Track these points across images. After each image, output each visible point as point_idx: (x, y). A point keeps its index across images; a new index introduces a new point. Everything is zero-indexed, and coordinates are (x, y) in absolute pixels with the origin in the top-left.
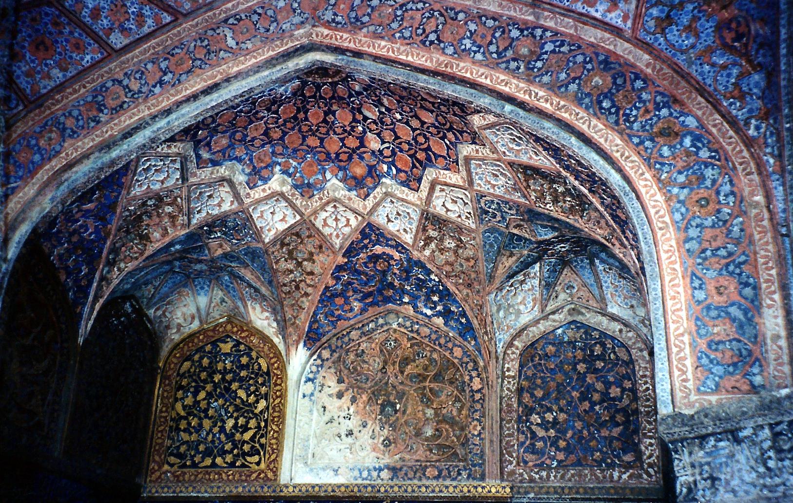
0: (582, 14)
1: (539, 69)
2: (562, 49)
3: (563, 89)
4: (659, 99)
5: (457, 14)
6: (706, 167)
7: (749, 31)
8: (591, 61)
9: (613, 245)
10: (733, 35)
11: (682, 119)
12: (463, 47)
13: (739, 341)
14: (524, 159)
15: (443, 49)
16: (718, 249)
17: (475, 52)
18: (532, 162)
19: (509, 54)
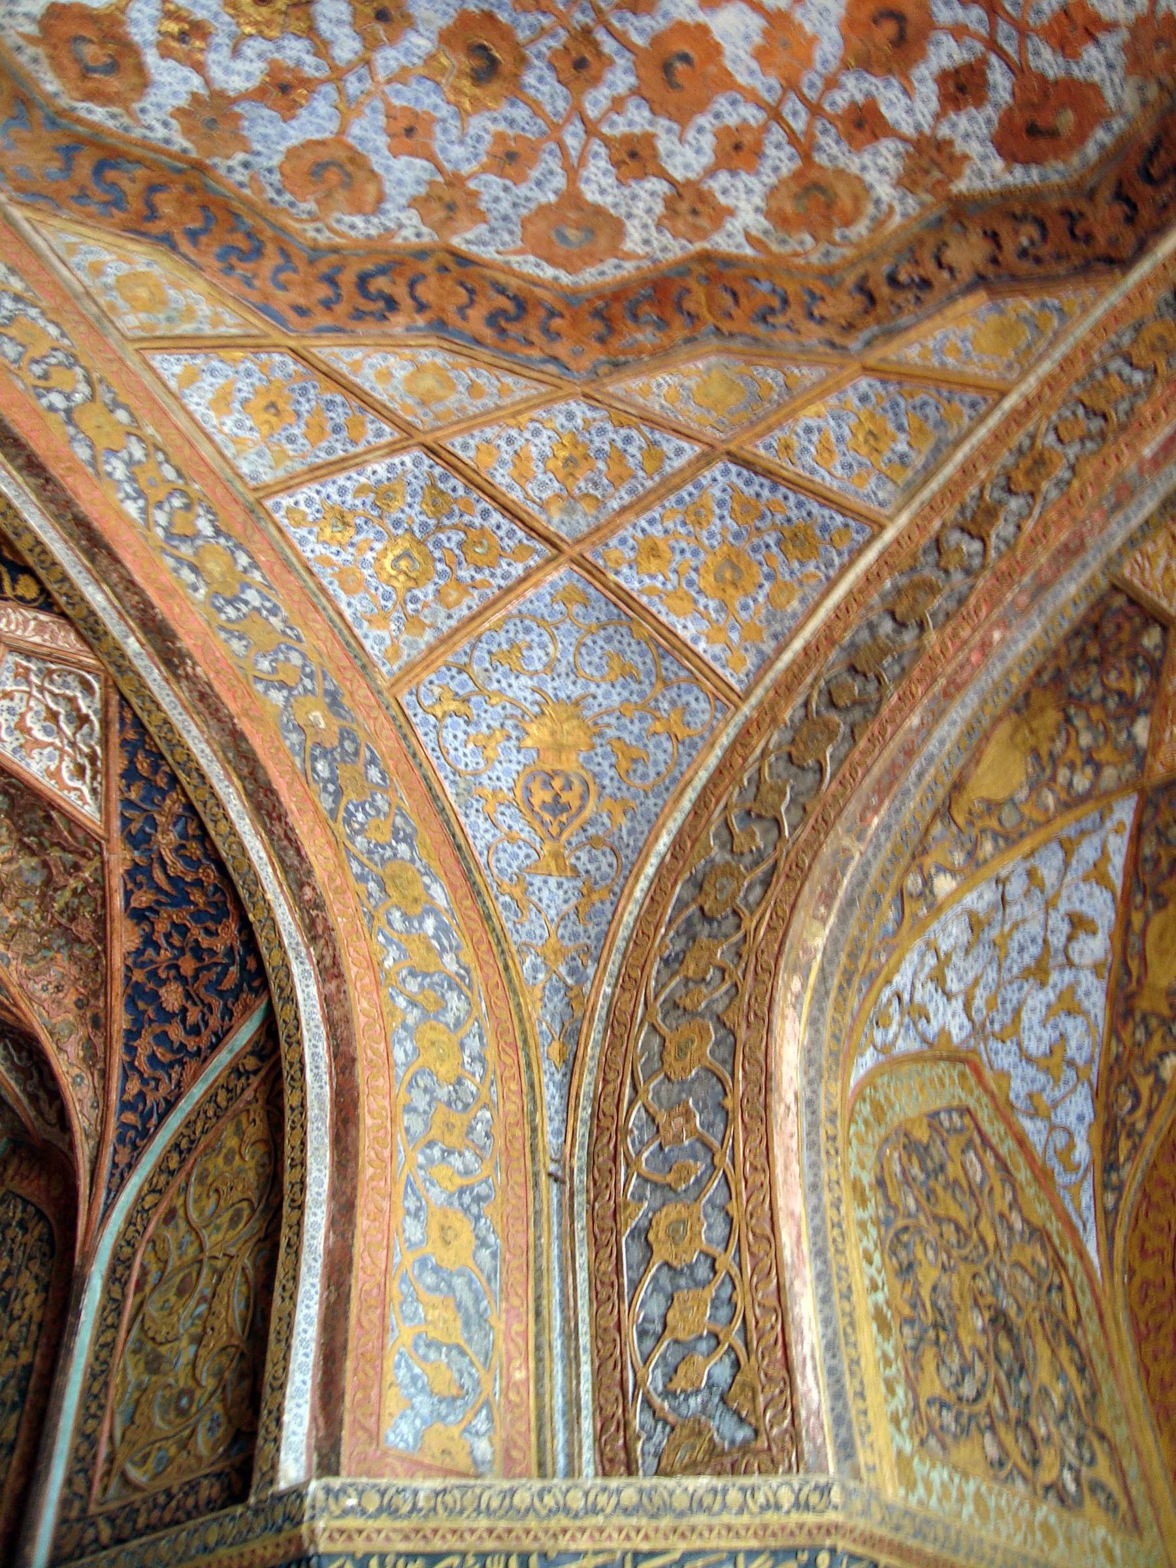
0: (323, 590)
1: (229, 620)
2: (272, 619)
3: (260, 687)
4: (399, 820)
5: (116, 405)
6: (450, 988)
7: (581, 808)
8: (311, 676)
9: (60, 1049)
10: (548, 797)
11: (427, 880)
12: (109, 468)
13: (463, 1353)
14: (34, 767)
15: (72, 439)
16: (450, 1153)
17: (128, 497)
18: (48, 785)
19: (186, 550)
